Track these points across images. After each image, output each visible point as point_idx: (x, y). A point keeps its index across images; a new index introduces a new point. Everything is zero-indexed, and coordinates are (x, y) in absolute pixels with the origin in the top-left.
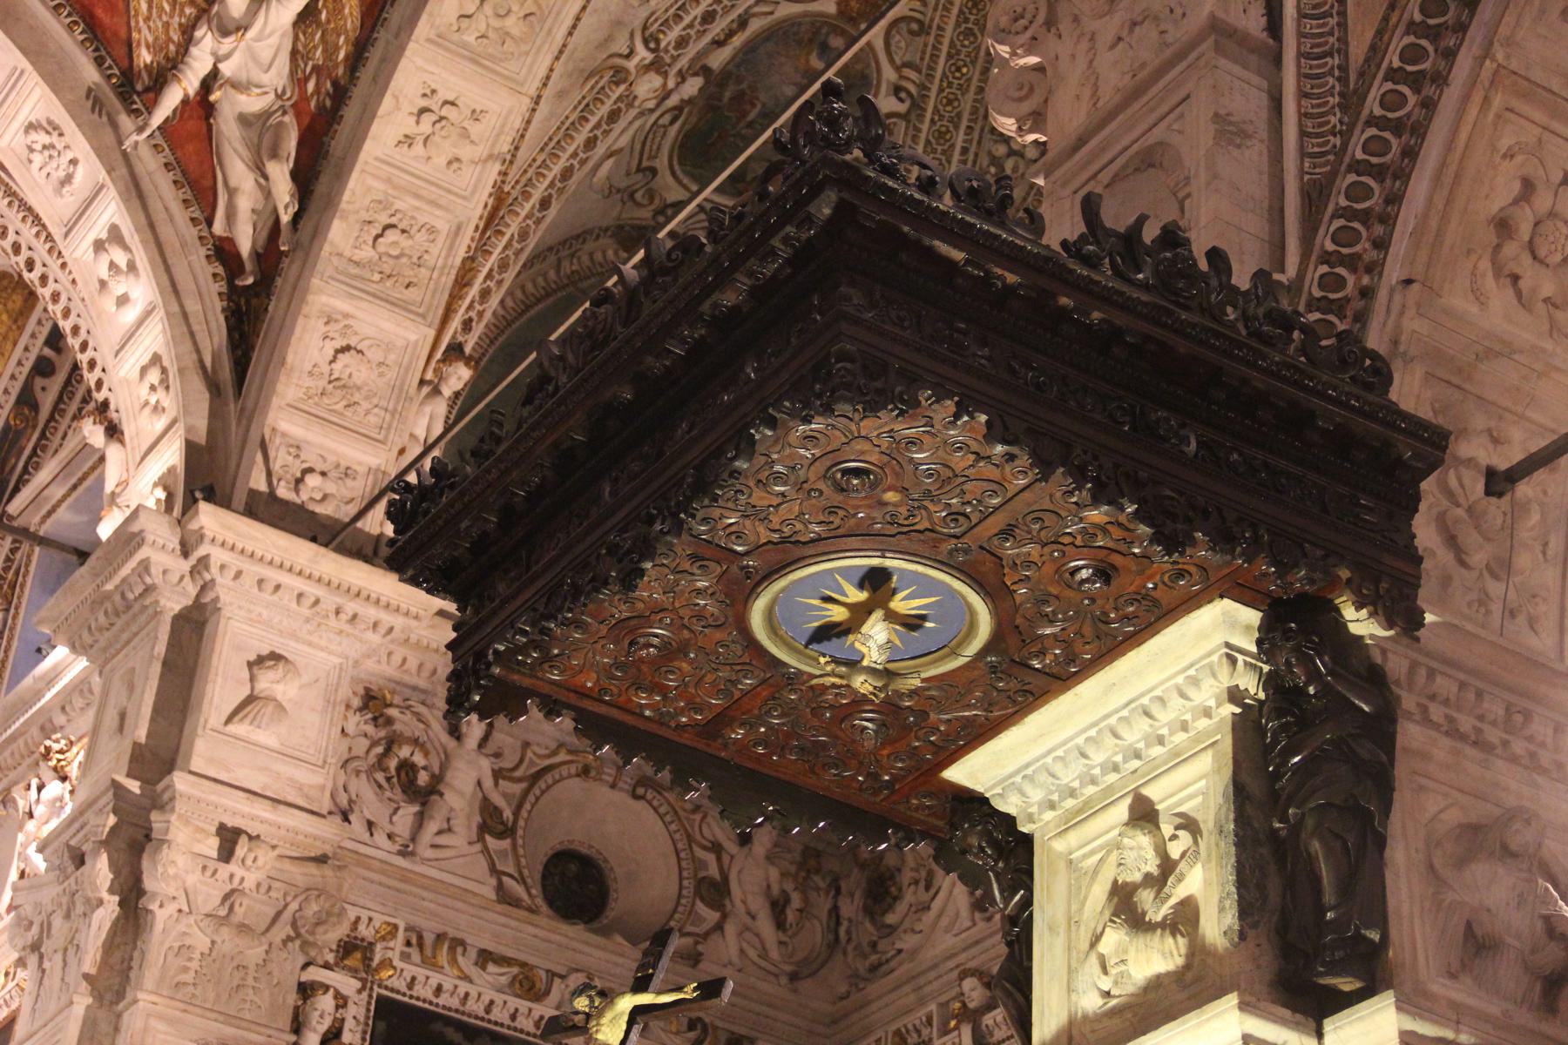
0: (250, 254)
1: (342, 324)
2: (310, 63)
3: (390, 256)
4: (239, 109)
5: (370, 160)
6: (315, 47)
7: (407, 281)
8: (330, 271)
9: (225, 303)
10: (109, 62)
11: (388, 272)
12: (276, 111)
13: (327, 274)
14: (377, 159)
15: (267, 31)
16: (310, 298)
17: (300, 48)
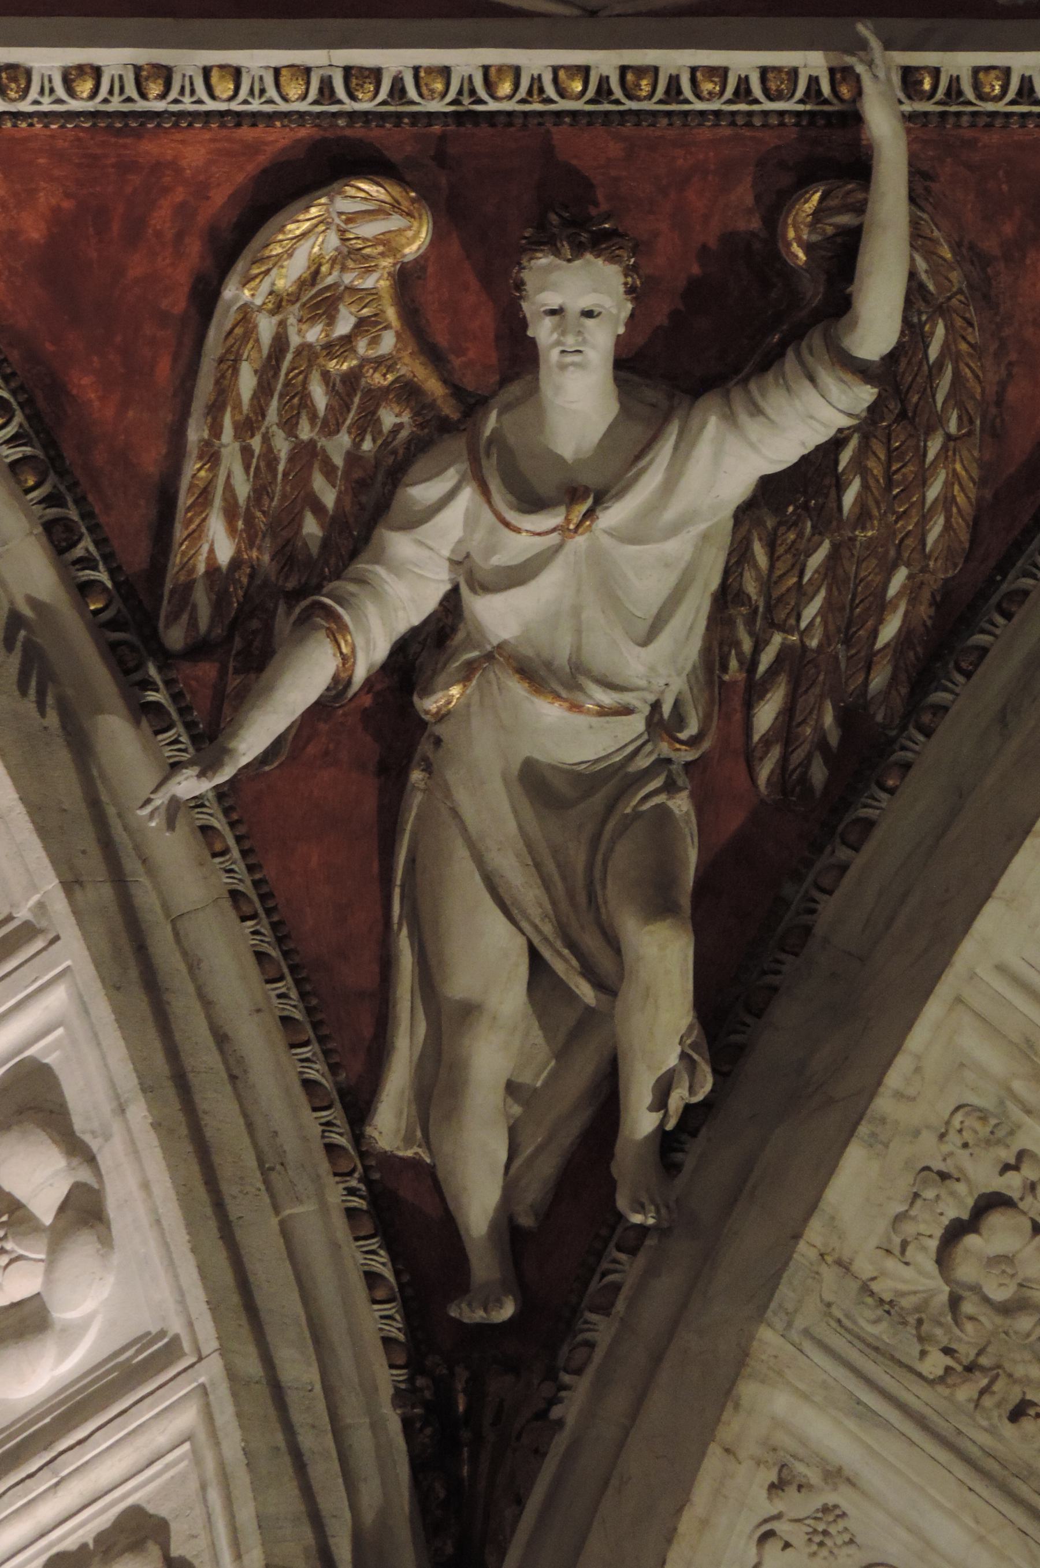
0: (494, 1226)
1: (818, 1503)
2: (777, 639)
3: (986, 1300)
4: (527, 749)
5: (986, 973)
6: (802, 594)
7: (1015, 1398)
8: (809, 1316)
9: (401, 1374)
10: (86, 546)
11: (967, 1352)
12: (647, 774)
13: (800, 1323)
14: (1001, 969)
15: (669, 515)
16: (748, 1390)
17: (751, 587)
